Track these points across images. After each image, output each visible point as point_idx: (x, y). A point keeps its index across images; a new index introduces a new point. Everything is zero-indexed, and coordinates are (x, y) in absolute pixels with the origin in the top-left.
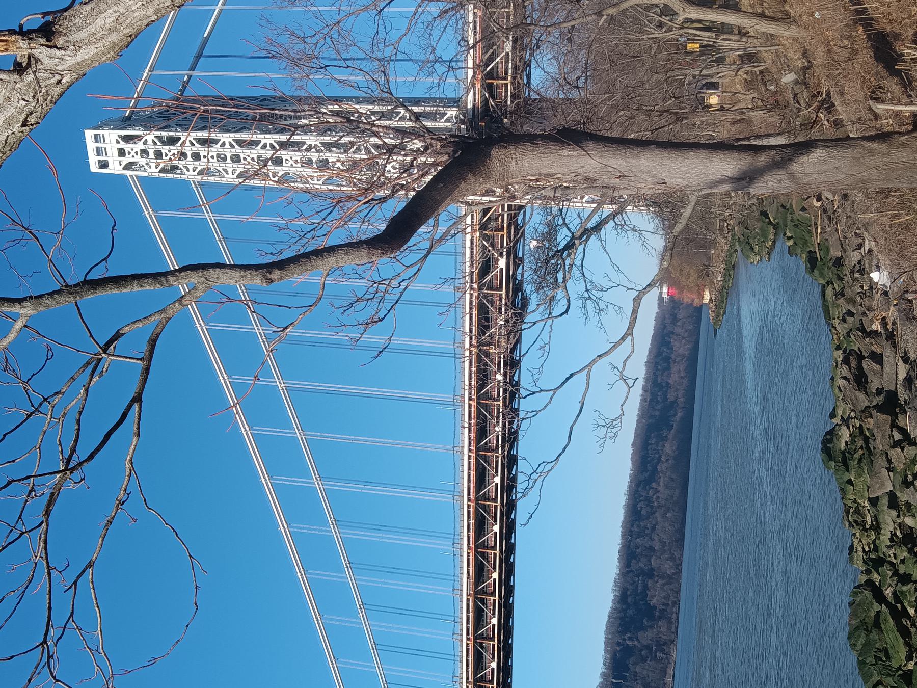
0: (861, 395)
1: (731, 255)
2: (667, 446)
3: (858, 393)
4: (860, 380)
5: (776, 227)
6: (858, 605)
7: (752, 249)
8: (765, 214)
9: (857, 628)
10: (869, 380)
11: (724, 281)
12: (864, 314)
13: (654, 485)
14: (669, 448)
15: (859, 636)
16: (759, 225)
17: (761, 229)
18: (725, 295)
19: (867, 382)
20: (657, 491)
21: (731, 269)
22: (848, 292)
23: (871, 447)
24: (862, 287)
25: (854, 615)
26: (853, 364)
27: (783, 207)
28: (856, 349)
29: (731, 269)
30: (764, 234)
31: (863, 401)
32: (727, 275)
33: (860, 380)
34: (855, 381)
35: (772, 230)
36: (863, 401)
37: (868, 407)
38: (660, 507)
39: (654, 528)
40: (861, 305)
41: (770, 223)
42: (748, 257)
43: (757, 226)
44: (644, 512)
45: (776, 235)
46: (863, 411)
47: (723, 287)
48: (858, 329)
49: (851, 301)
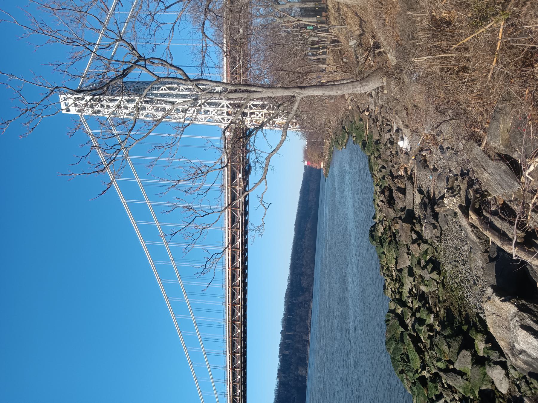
0: (391, 211)
1: (331, 148)
2: (308, 224)
3: (389, 209)
4: (391, 202)
5: (348, 133)
6: (391, 326)
7: (339, 144)
8: (344, 128)
9: (390, 339)
10: (396, 202)
11: (329, 159)
12: (393, 166)
13: (303, 240)
14: (309, 225)
15: (392, 344)
16: (341, 132)
17: (342, 134)
18: (329, 164)
19: (394, 204)
20: (304, 242)
21: (331, 154)
22: (383, 156)
23: (397, 239)
24: (391, 152)
25: (388, 331)
26: (387, 193)
27: (351, 122)
28: (387, 185)
29: (331, 154)
30: (344, 137)
31: (392, 214)
32: (330, 156)
33: (391, 202)
34: (388, 203)
35: (346, 134)
36: (392, 214)
37: (396, 217)
38: (305, 248)
39: (303, 257)
40: (391, 161)
41: (346, 131)
42: (337, 147)
43: (340, 133)
44: (299, 250)
45: (348, 137)
46: (393, 220)
47: (328, 161)
48: (389, 175)
49: (385, 161)
